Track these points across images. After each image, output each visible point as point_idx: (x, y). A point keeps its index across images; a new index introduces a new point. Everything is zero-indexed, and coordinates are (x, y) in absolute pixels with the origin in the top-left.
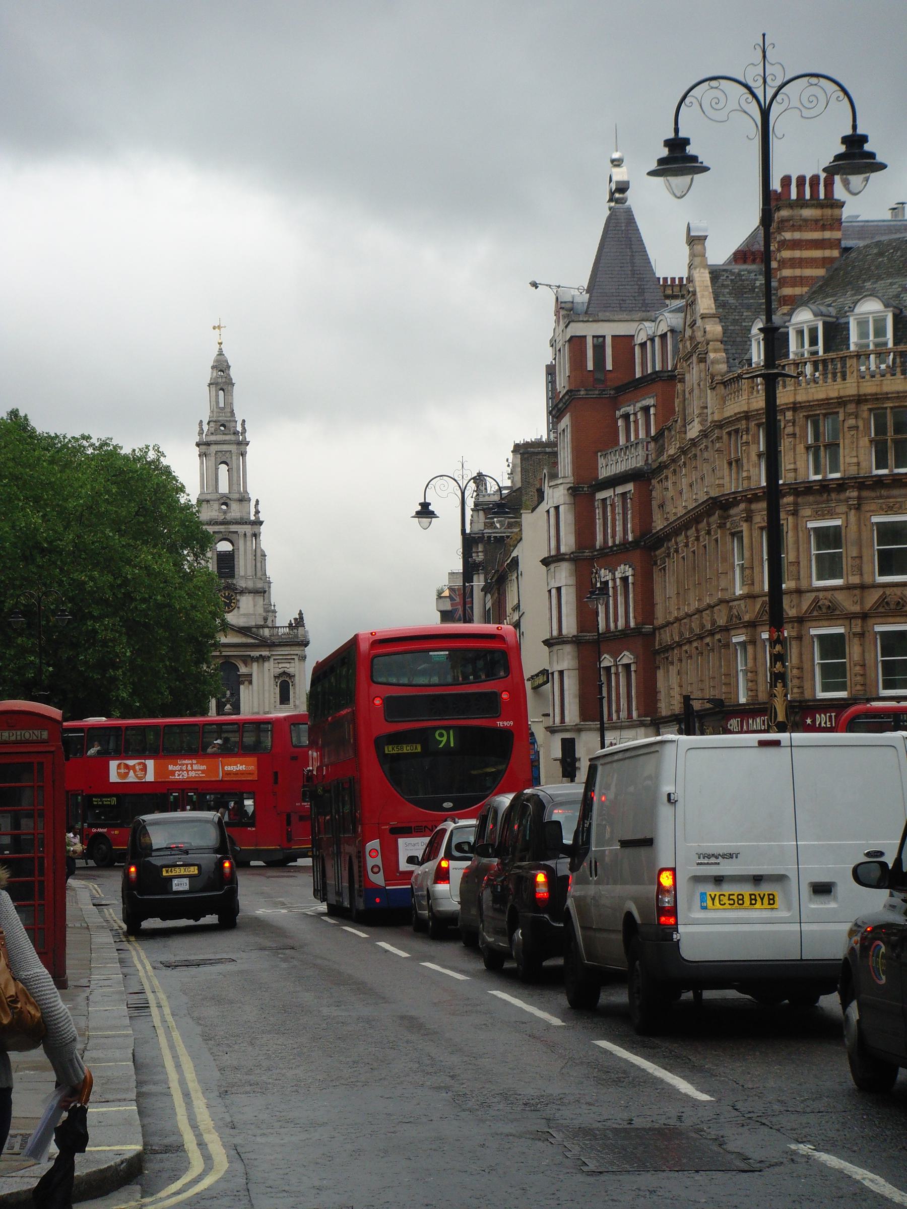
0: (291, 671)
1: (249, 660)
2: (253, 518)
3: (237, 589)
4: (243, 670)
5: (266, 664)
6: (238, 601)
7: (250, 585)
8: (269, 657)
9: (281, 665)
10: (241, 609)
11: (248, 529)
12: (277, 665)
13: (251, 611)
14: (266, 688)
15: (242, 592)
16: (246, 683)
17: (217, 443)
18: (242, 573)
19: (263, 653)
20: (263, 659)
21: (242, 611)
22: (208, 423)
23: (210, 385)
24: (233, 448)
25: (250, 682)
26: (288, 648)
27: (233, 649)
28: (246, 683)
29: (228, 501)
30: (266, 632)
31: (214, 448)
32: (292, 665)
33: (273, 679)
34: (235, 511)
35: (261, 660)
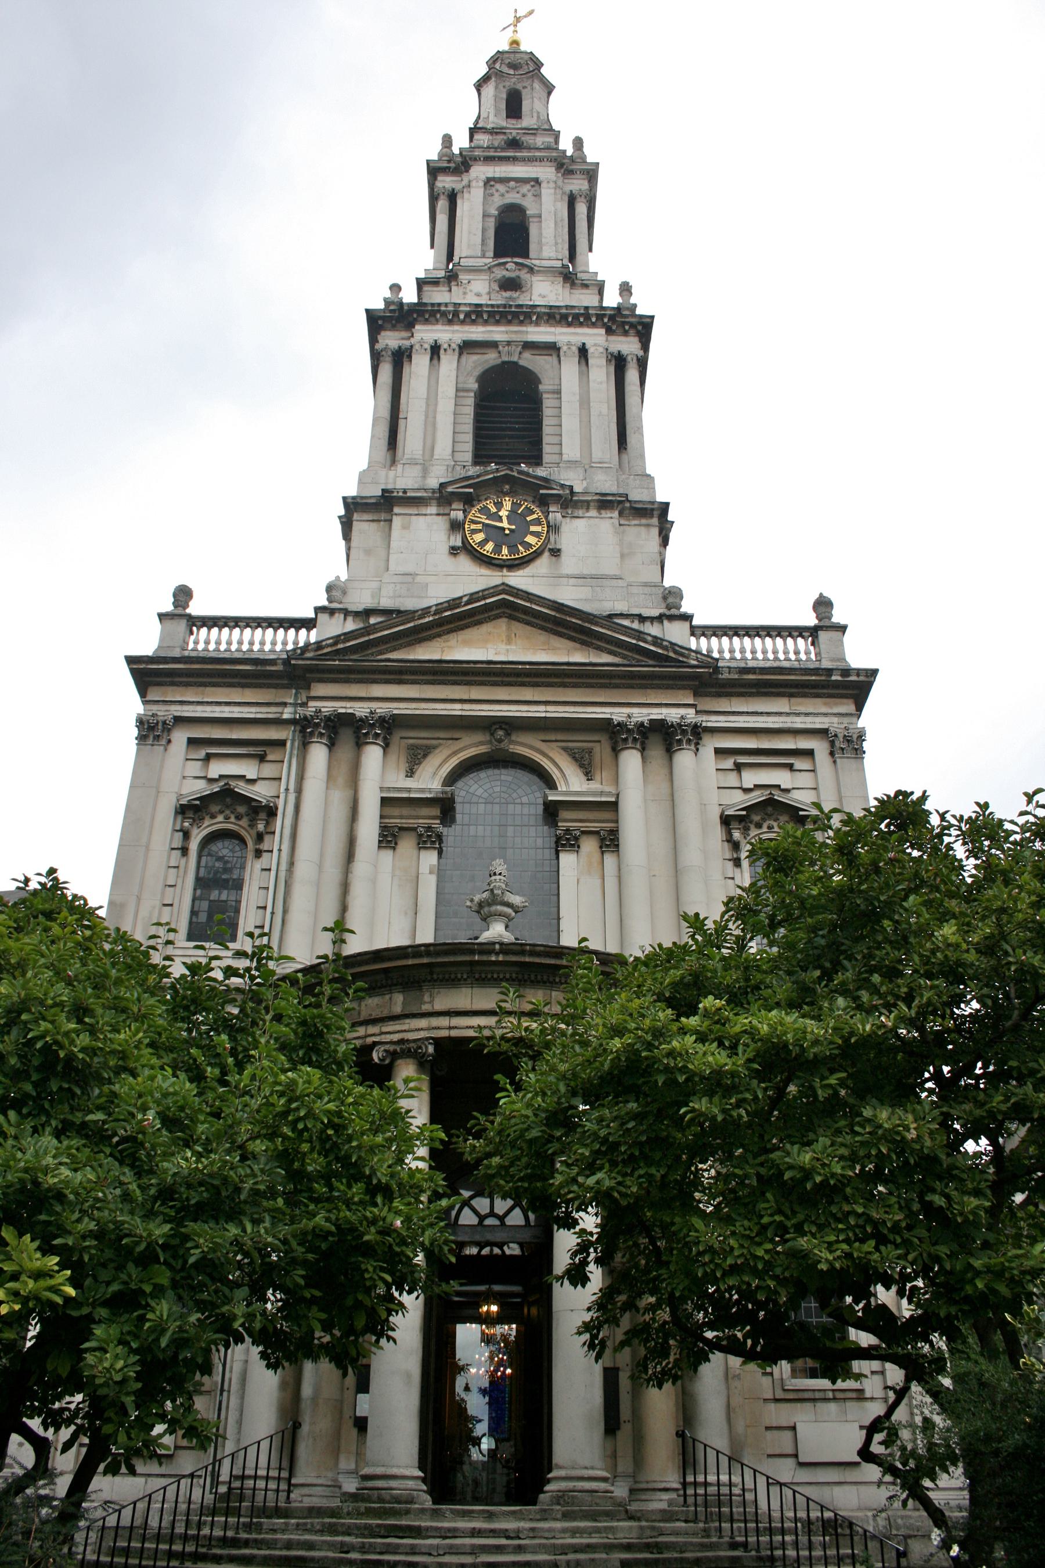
0: (802, 798)
1: (601, 749)
2: (612, 299)
3: (547, 482)
4: (572, 784)
5: (684, 758)
6: (554, 528)
7: (605, 483)
8: (697, 733)
9: (750, 778)
10: (564, 556)
11: (594, 338)
12: (732, 779)
13: (610, 567)
14: (692, 855)
15: (570, 501)
16: (589, 846)
17: (489, 160)
18: (571, 450)
19: (673, 715)
20: (665, 738)
21: (569, 564)
22: (473, 132)
23: (479, 86)
24: (546, 172)
25: (610, 841)
26: (781, 705)
27: (528, 694)
28: (589, 846)
29: (524, 275)
30: (675, 633)
31: (480, 172)
32: (804, 780)
33: (717, 832)
34: (545, 292)
35: (656, 752)
